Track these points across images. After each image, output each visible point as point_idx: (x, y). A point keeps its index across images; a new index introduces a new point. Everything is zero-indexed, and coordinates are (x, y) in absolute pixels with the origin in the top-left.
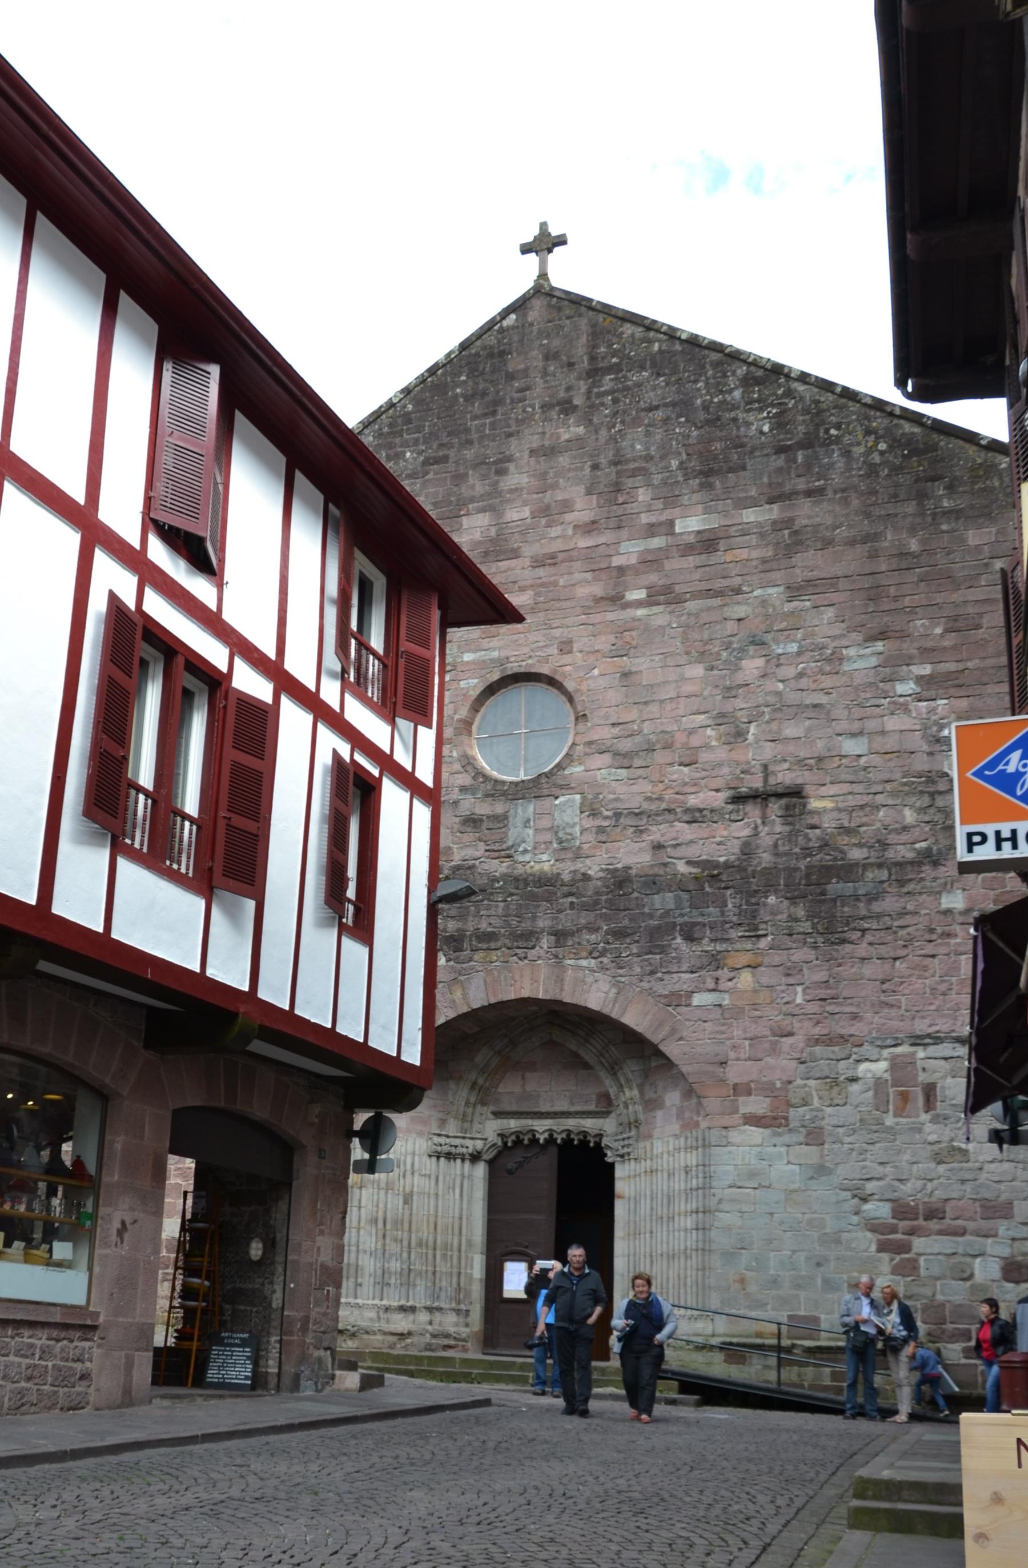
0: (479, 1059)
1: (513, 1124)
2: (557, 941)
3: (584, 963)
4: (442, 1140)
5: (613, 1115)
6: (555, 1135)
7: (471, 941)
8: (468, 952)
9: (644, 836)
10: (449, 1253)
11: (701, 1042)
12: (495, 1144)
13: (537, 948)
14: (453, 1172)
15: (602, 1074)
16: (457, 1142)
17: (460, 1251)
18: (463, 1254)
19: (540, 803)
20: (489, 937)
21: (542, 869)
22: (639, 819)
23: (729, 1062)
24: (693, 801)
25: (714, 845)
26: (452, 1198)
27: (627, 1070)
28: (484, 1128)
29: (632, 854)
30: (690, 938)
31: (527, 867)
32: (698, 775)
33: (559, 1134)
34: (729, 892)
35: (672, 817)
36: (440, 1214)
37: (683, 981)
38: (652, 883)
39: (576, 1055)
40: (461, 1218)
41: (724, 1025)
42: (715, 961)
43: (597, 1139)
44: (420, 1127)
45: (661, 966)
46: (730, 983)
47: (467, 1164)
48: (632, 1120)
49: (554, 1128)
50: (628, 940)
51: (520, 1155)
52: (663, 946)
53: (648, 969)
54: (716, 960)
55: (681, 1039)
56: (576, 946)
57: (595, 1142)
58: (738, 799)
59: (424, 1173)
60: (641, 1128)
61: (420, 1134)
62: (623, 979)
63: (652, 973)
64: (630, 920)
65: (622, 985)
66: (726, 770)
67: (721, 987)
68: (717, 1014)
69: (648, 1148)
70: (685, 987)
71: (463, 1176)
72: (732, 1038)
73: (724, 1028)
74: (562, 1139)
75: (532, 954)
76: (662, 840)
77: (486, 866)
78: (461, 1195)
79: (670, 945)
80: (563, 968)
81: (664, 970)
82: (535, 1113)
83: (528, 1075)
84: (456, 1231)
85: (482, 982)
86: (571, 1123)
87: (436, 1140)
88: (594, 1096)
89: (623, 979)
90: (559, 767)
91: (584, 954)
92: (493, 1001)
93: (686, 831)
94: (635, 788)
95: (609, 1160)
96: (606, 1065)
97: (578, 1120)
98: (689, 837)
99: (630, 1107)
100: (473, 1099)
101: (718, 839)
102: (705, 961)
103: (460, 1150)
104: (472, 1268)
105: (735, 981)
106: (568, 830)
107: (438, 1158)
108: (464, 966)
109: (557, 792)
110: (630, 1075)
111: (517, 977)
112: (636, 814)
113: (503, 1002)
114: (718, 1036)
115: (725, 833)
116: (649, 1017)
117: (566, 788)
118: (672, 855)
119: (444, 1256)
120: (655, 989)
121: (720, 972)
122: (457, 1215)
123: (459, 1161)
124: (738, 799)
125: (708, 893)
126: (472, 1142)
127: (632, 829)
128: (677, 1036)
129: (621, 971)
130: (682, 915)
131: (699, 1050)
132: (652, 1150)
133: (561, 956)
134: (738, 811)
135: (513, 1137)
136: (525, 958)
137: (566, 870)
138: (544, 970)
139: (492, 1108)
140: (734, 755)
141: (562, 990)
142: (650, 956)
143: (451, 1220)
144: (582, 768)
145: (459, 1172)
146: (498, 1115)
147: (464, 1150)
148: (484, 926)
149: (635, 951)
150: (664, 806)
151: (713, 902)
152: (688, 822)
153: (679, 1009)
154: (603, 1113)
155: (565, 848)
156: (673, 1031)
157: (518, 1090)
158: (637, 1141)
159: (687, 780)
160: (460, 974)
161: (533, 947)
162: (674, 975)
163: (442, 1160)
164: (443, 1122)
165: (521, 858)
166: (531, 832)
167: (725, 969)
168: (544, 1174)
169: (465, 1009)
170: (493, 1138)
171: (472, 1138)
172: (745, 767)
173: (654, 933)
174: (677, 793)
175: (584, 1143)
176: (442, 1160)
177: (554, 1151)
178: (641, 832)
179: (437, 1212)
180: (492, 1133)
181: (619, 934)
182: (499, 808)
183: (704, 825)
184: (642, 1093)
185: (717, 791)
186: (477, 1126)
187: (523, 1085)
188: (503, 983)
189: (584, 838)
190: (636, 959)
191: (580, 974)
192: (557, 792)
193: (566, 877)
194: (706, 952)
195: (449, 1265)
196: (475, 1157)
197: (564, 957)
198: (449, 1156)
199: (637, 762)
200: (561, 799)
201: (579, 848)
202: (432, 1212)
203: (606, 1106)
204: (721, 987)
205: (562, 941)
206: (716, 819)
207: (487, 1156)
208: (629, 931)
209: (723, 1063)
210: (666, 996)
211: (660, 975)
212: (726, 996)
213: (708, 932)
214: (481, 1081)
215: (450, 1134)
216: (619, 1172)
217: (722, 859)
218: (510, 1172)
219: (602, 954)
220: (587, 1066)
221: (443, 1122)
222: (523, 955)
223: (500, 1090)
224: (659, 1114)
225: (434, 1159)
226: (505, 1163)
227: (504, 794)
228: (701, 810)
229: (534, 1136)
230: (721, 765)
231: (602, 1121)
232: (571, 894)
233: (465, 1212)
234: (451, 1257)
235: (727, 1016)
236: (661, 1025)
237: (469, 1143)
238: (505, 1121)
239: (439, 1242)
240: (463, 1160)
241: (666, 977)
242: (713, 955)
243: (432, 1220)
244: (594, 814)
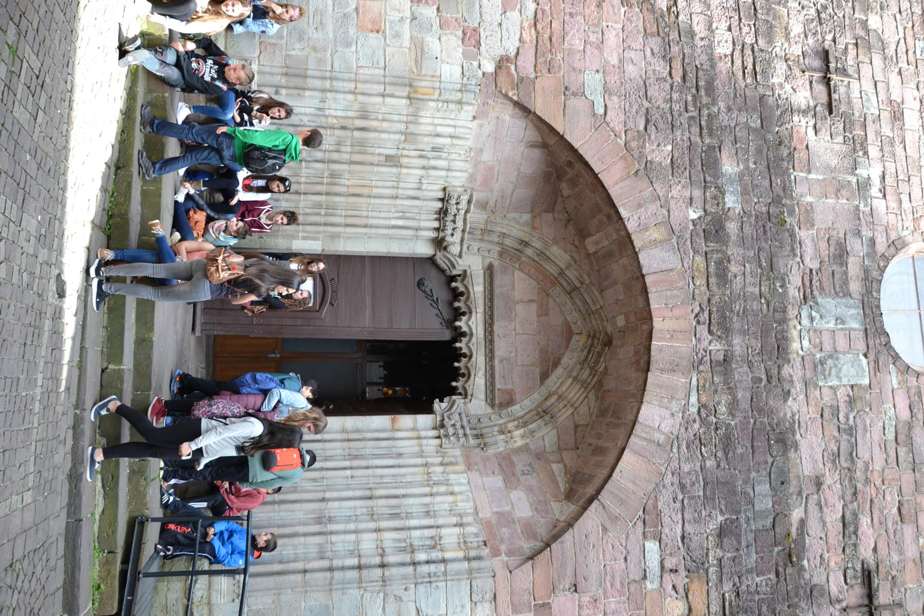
0: (556, 251)
1: (478, 289)
2: (718, 363)
3: (694, 399)
4: (463, 205)
5: (489, 410)
6: (465, 340)
7: (718, 251)
8: (705, 249)
9: (829, 465)
10: (323, 211)
11: (601, 556)
12: (454, 267)
13: (710, 337)
14: (423, 217)
15: (536, 397)
16: (460, 224)
17: (325, 224)
18: (322, 228)
19: (861, 335)
20: (723, 276)
21: (794, 341)
22: (845, 457)
23: (577, 595)
24: (865, 520)
25: (820, 551)
26: (392, 215)
27: (545, 430)
28: (474, 254)
29: (810, 453)
30: (722, 533)
31: (796, 322)
32: (890, 525)
33: (467, 345)
34: (772, 576)
35: (848, 498)
36: (373, 201)
37: (672, 530)
38: (780, 481)
39: (556, 364)
40: (366, 226)
41: (622, 584)
42: (696, 567)
43: (460, 390)
44: (479, 178)
45: (691, 498)
46: (671, 587)
47: (433, 234)
48: (487, 440)
49: (474, 339)
50: (720, 454)
51: (442, 294)
52: (714, 500)
53: (687, 481)
54: (698, 568)
55: (605, 529)
56: (713, 388)
57: (456, 388)
58: (867, 577)
59: (424, 181)
60: (477, 450)
61: (472, 178)
62: (675, 450)
63: (682, 487)
64: (742, 455)
65: (669, 448)
66: (895, 558)
67: (667, 577)
68: (636, 575)
69: (457, 468)
70: (666, 530)
71: (417, 229)
72: (606, 597)
73: (618, 584)
74: (461, 348)
75: (703, 330)
76: (825, 487)
77: (795, 268)
78: (394, 227)
79: (714, 508)
80: (687, 373)
81: (686, 502)
82: (492, 317)
83: (534, 307)
84: (350, 221)
85: (670, 266)
86: (479, 360)
87: (465, 198)
88: (510, 387)
89: (675, 450)
90: (896, 358)
91: (704, 399)
92: (648, 280)
93: (833, 517)
94: (876, 450)
95: (437, 405)
96: (548, 403)
97: (483, 368)
98: (828, 520)
99: (503, 437)
100: (508, 242)
101: (826, 556)
102: (697, 554)
103: (450, 226)
104: (304, 238)
105: (673, 593)
106: (834, 371)
107: (442, 200)
108: (688, 243)
109: (872, 356)
110: (539, 435)
111: (676, 312)
112: (851, 454)
114: (608, 577)
115: (832, 564)
116: (631, 486)
117: (877, 367)
118: (810, 502)
119: (319, 205)
120: (664, 491)
121: (683, 573)
122: (371, 222)
123: (436, 224)
124: (867, 577)
125: (771, 551)
126: (458, 241)
127: (835, 449)
128: (608, 524)
129: (684, 447)
130: (748, 520)
131: (592, 554)
132: (455, 473)
133: (701, 368)
134: (855, 577)
135: (462, 289)
136: (698, 322)
137: (793, 371)
138: (684, 347)
139: (496, 263)
140: (910, 566)
141: (662, 370)
142: (702, 483)
143: (365, 214)
144: (896, 386)
145: (423, 224)
146: (490, 271)
147: (449, 232)
148: (734, 268)
149: (709, 463)
150: (860, 486)
151: (762, 558)
152: (843, 517)
153: (640, 524)
154: (493, 399)
155: (818, 367)
156: (614, 519)
157: (517, 295)
158: (463, 446)
159: (885, 512)
160: (679, 237)
161: (710, 332)
162: (680, 516)
163: (439, 205)
164: (483, 206)
165: (804, 313)
166: (831, 325)
167: (687, 580)
168: (418, 323)
169: (637, 244)
170: (461, 265)
171: (462, 240)
172: (898, 581)
173: (728, 487)
174: (871, 501)
175: (456, 374)
176: (439, 205)
177: (446, 335)
178: (834, 461)
179: (375, 197)
180: (467, 264)
181: (727, 443)
182: (855, 286)
183: (841, 538)
184: (519, 450)
185: (875, 550)
186: (475, 245)
187: (522, 301)
188: (669, 293)
189: (826, 391)
190: (698, 464)
191: (681, 394)
192: (872, 356)
193: (786, 370)
194: (707, 554)
195: (308, 211)
196: (439, 243)
197: (700, 372)
198: (442, 213)
199: (902, 451)
200: (864, 361)
201: (816, 386)
202: (375, 191)
203: (500, 401)
204: (667, 577)
205: (718, 369)
206: (848, 551)
207: (439, 258)
208: (730, 455)
209: (575, 588)
210: (655, 506)
211: (680, 497)
212: (656, 585)
213: (729, 555)
214: (529, 252)
215: (468, 215)
216: (424, 420)
217: (805, 563)
218: (420, 284)
219: (703, 422)
220: (544, 376)
221: (483, 206)
222: (702, 319)
223: (517, 273)
225: (440, 195)
226: (434, 277)
227: (869, 292)
228: (855, 533)
229: (464, 314)
230: (901, 552)
231: (483, 397)
232: (769, 379)
233: (373, 231)
234: (319, 214)
235: (632, 588)
236: (622, 502)
237: (458, 236)
238: (481, 280)
239: (337, 199)
240: (437, 229)
241: (678, 505)
242: (703, 564)
243: (365, 191)
244: (851, 402)
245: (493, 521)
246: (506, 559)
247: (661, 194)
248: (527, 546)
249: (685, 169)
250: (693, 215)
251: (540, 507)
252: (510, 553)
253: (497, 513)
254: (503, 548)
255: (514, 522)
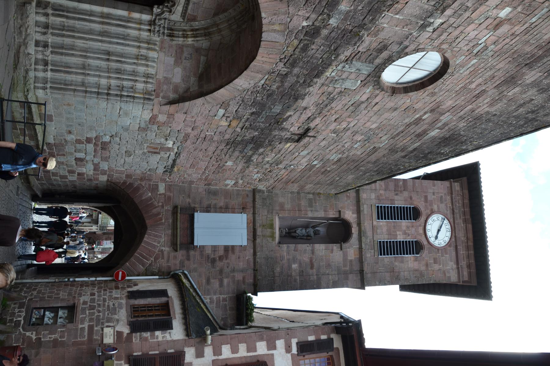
108: (294, 35)
113: (259, 46)
169: (264, 28)
224: (171, 60)
245: (162, 81)
246: (161, 99)
247: (291, 12)
248: (172, 96)
249: (314, 4)
250: (305, 24)
251: (185, 79)
252: (163, 98)
253: (165, 77)
254: (161, 94)
255: (171, 83)
